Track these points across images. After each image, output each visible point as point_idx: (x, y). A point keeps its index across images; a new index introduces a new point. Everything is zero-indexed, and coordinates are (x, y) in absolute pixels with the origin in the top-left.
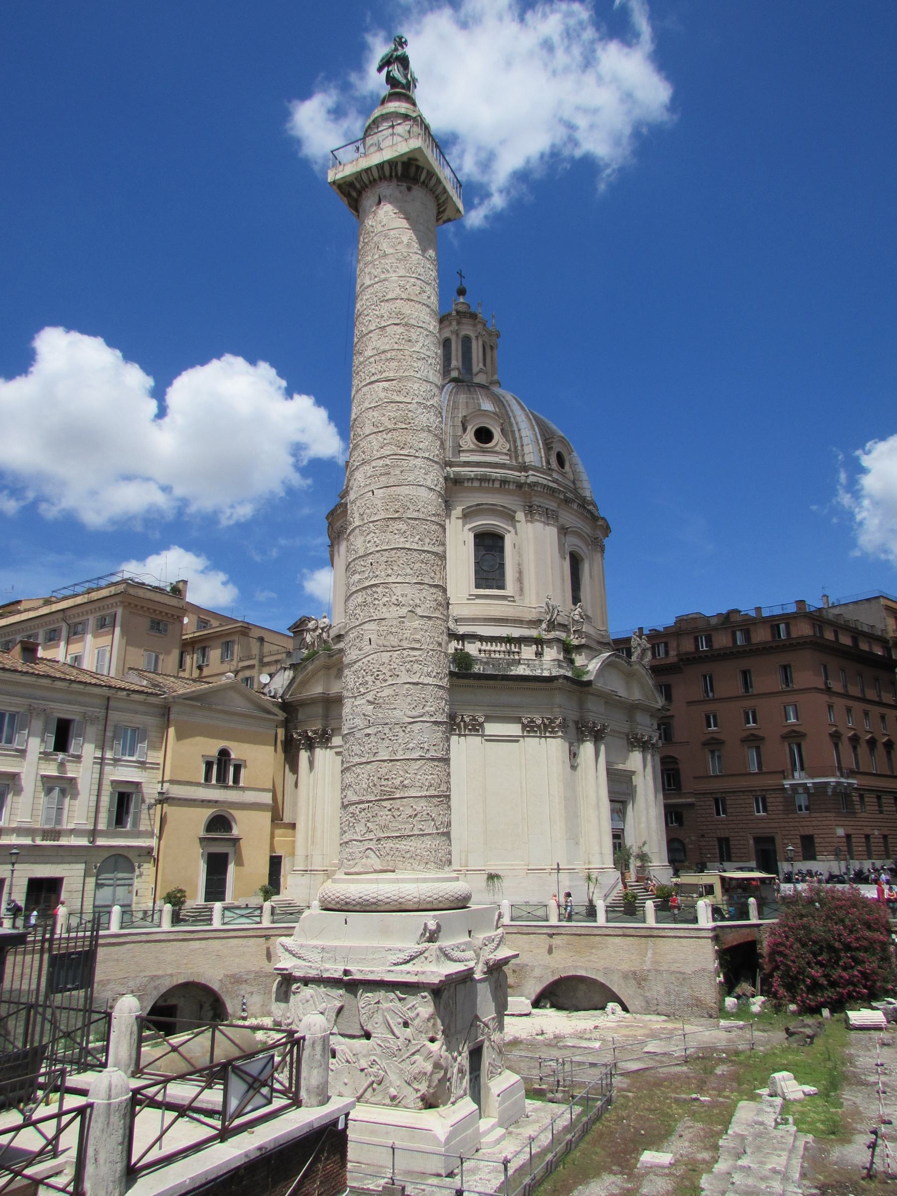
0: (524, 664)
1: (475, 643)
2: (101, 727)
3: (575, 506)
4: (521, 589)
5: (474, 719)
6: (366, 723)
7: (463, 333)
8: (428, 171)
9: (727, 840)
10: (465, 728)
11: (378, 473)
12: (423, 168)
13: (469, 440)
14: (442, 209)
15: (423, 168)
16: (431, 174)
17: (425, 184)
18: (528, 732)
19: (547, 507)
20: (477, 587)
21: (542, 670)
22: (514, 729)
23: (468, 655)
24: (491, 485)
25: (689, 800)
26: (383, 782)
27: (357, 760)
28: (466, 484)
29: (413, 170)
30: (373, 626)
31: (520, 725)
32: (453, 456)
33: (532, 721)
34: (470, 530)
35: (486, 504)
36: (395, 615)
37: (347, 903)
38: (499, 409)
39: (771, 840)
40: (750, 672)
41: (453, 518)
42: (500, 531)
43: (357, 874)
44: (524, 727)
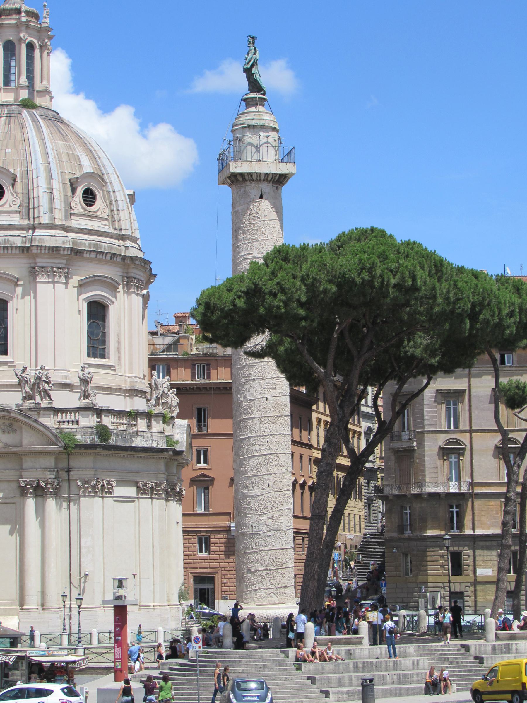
0: (141, 436)
1: (108, 416)
4: (119, 359)
5: (109, 484)
6: (268, 529)
10: (102, 490)
11: (269, 387)
18: (142, 494)
20: (89, 356)
22: (131, 492)
24: (104, 257)
26: (278, 560)
27: (262, 548)
28: (85, 255)
30: (270, 477)
31: (135, 489)
32: (66, 219)
33: (145, 485)
34: (84, 299)
35: (100, 276)
36: (280, 472)
37: (268, 619)
39: (211, 579)
40: (204, 410)
41: (70, 286)
42: (107, 302)
43: (265, 605)
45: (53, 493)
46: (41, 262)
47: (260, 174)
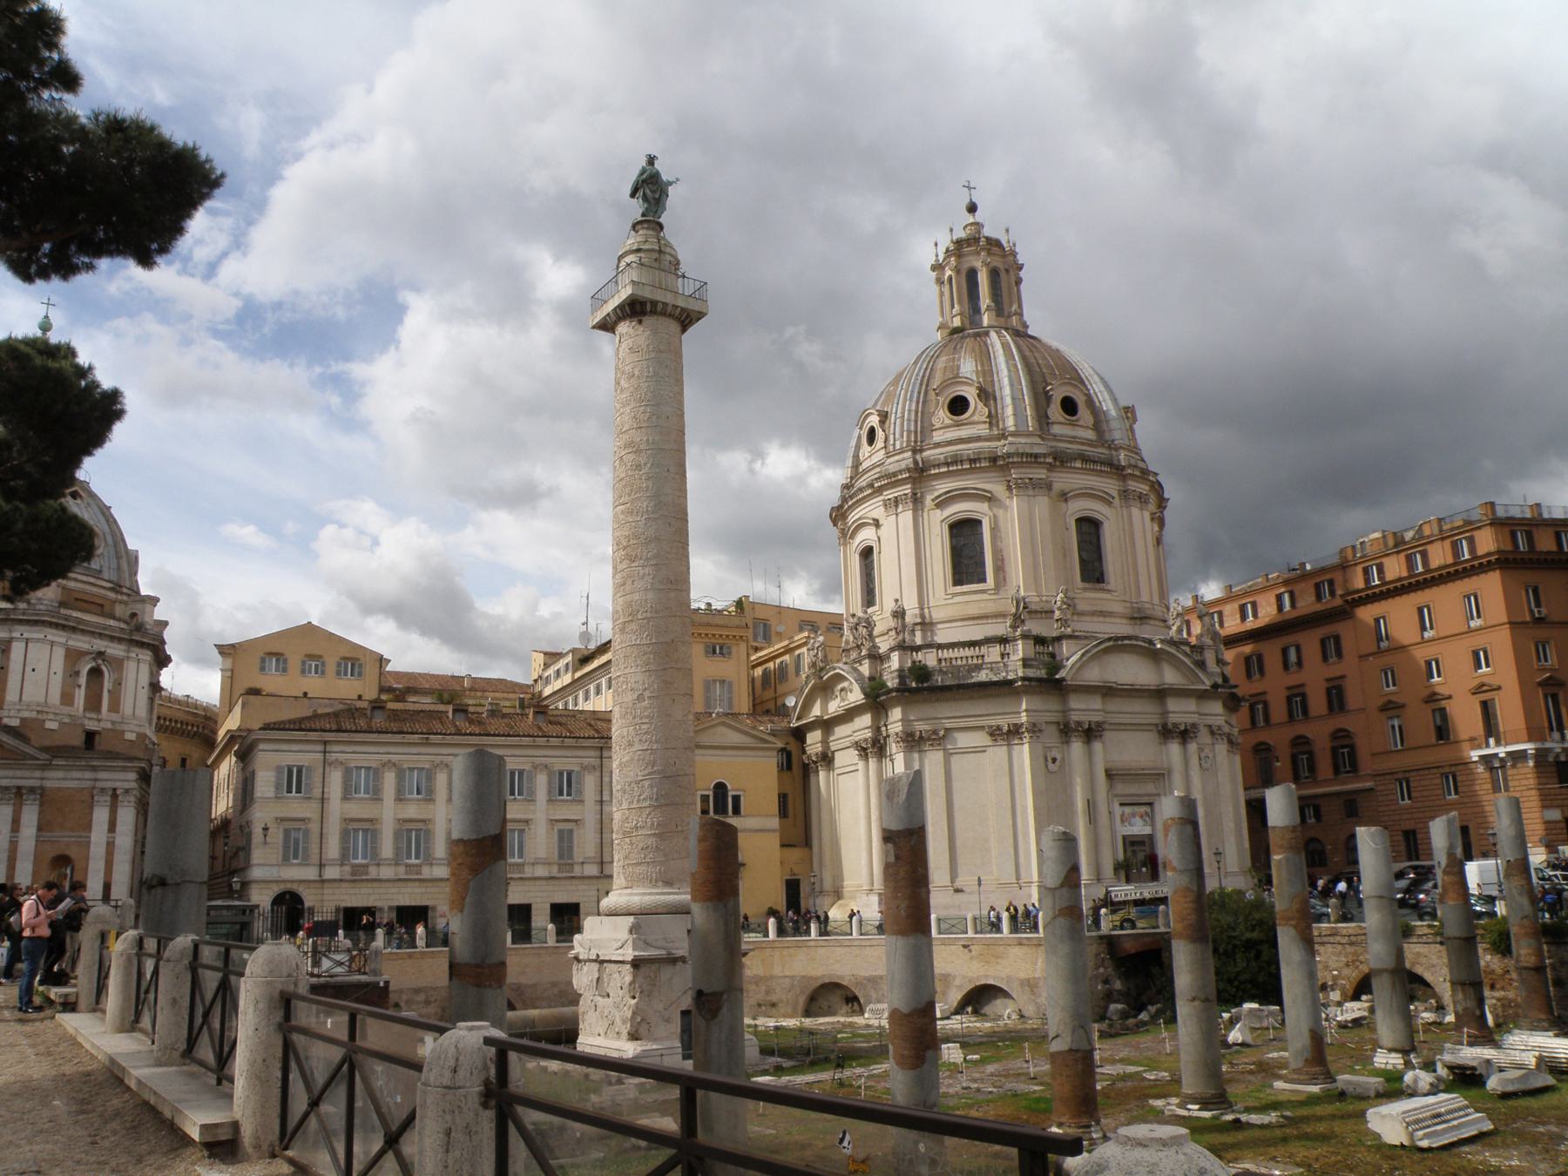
0: (987, 668)
2: (598, 774)
3: (1078, 464)
7: (965, 266)
9: (1414, 832)
12: (646, 303)
13: (942, 416)
15: (646, 303)
16: (654, 303)
17: (653, 312)
19: (1031, 476)
21: (1007, 672)
23: (925, 667)
25: (1368, 784)
29: (638, 307)
38: (982, 365)
44: (992, 735)
46: (890, 494)
47: (608, 315)
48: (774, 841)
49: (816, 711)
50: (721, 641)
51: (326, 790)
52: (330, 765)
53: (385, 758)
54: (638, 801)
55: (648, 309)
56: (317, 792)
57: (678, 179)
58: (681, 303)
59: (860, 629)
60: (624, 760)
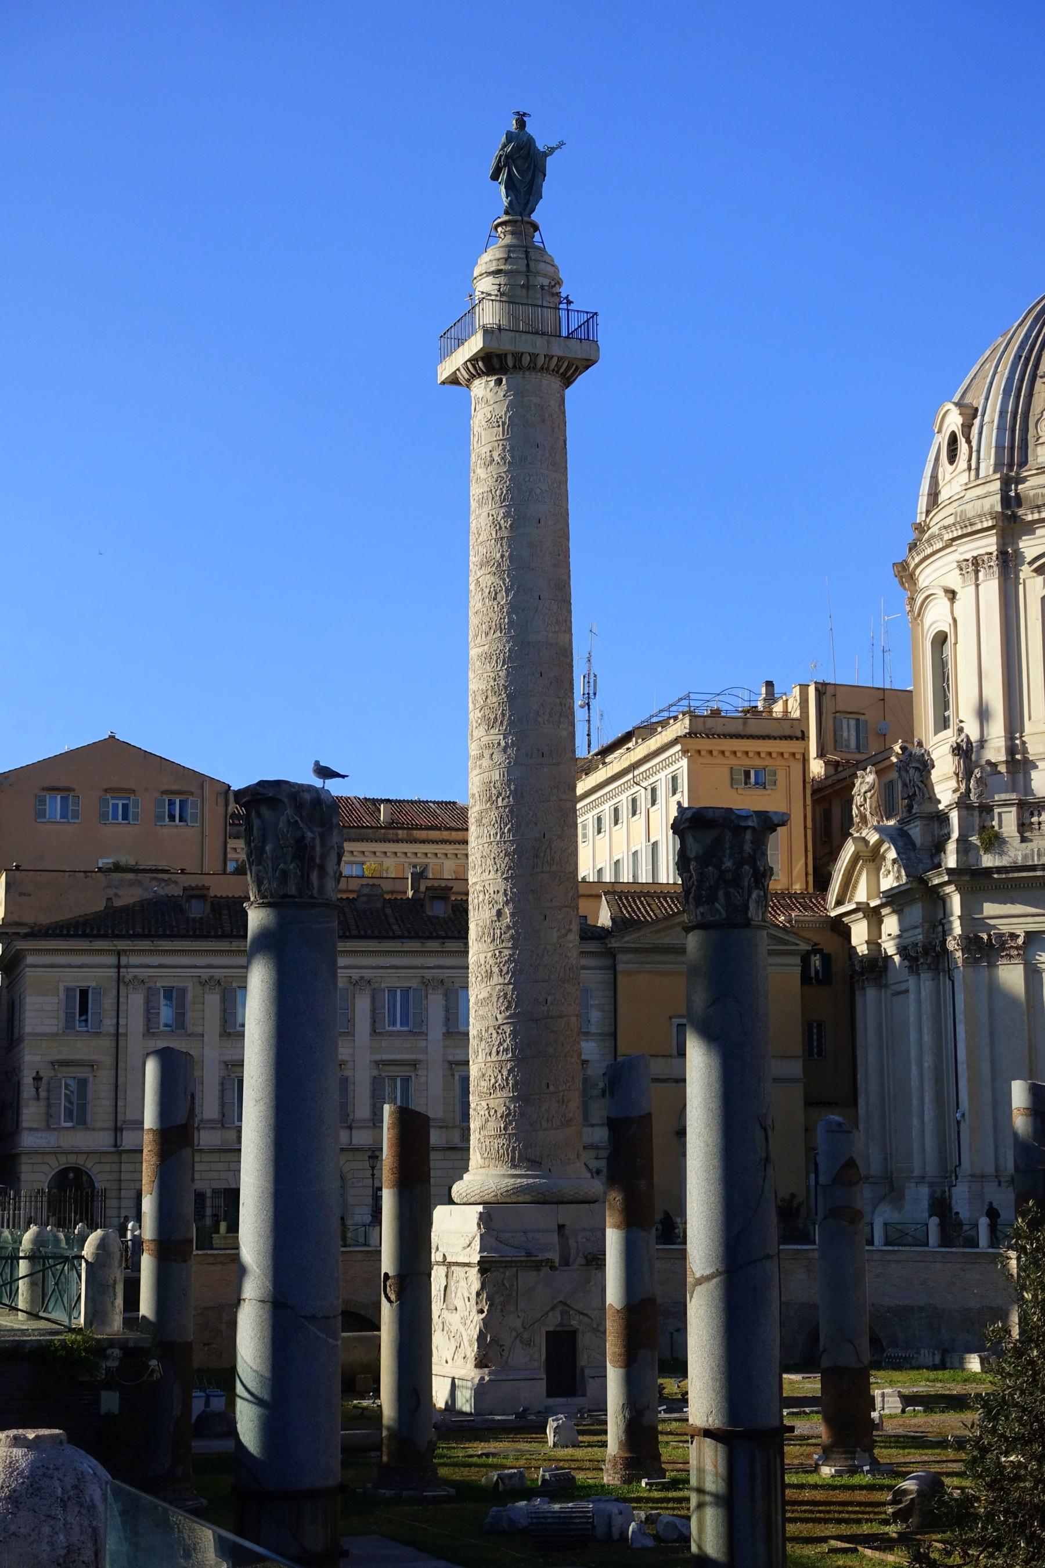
8: (513, 354)
12: (506, 355)
14: (561, 371)
15: (506, 355)
16: (518, 356)
17: (518, 367)
26: (483, 1083)
29: (495, 361)
45: (926, 967)
47: (458, 369)
48: (797, 1094)
49: (861, 894)
50: (758, 762)
51: (122, 1022)
52: (126, 984)
53: (205, 973)
54: (498, 1053)
55: (510, 362)
56: (108, 1025)
57: (561, 144)
58: (557, 349)
59: (912, 771)
60: (481, 997)
